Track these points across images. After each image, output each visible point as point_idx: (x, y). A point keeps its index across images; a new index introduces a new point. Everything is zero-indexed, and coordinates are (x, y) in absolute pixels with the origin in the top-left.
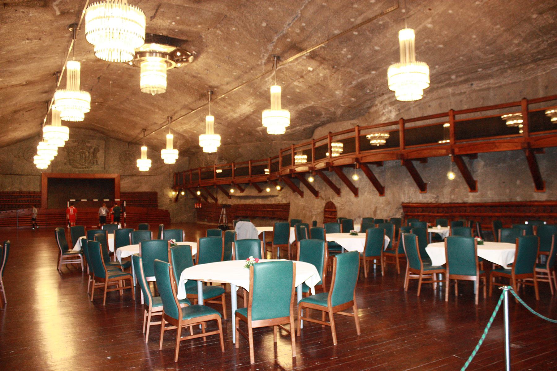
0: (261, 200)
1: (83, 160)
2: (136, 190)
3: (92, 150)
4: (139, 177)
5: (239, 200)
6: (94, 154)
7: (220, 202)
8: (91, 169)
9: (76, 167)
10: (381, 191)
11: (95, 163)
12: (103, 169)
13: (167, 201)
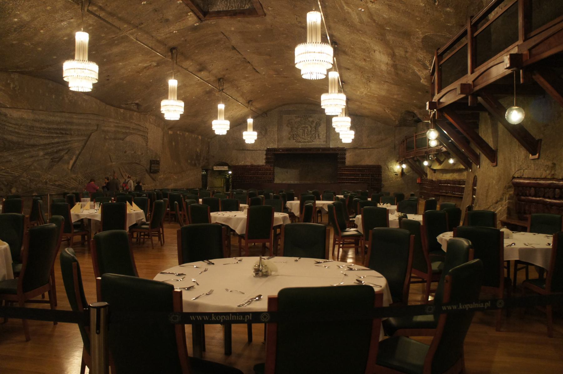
0: (457, 174)
1: (306, 135)
2: (359, 164)
3: (314, 124)
4: (362, 150)
5: (441, 174)
6: (315, 128)
7: (429, 177)
8: (313, 143)
9: (300, 142)
10: (492, 155)
11: (317, 138)
12: (325, 143)
13: (393, 175)
